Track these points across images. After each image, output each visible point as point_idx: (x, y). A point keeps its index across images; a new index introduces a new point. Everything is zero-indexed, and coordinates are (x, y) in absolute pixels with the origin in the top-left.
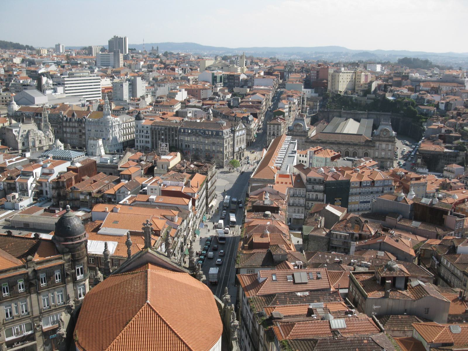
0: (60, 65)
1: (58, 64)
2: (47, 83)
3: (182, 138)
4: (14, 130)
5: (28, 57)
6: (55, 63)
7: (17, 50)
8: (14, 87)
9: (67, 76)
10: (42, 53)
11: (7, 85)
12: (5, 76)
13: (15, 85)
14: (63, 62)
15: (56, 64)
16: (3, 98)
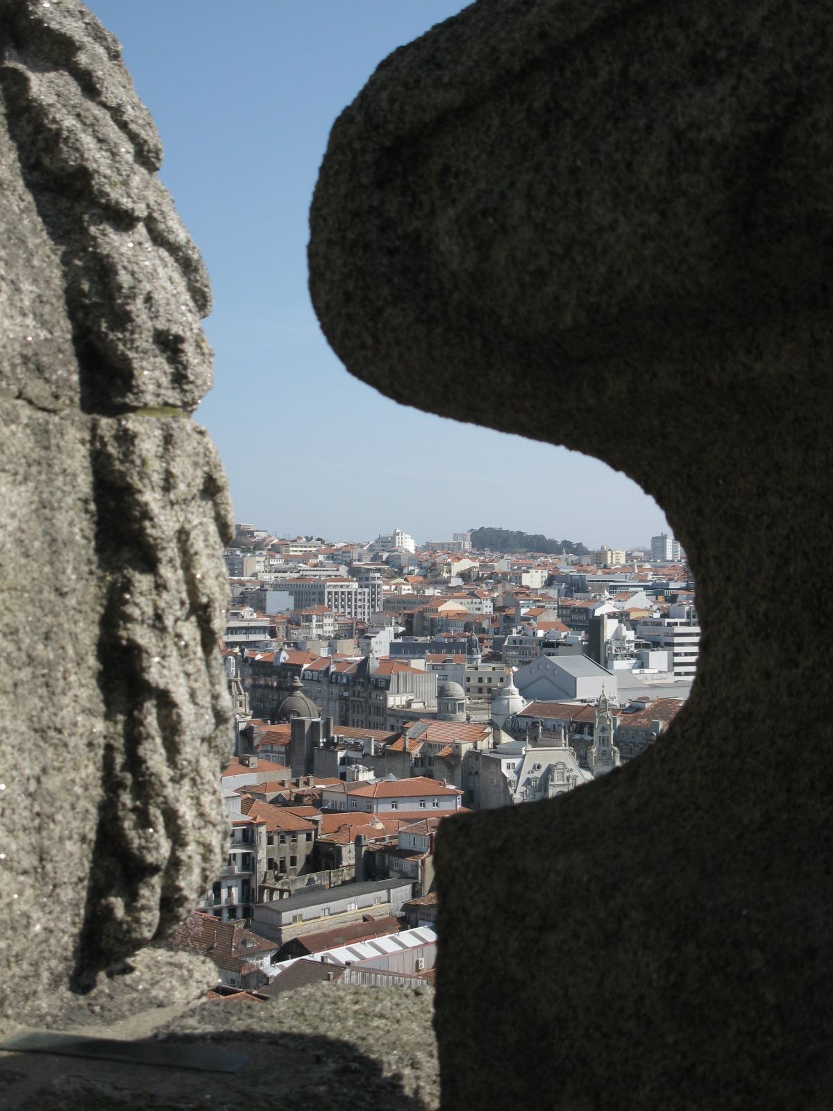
0: (661, 593)
1: (655, 590)
2: (618, 637)
4: (504, 762)
5: (566, 570)
6: (646, 588)
7: (535, 554)
8: (516, 648)
9: (684, 620)
10: (609, 561)
11: (497, 644)
12: (493, 620)
13: (521, 642)
14: (672, 585)
15: (650, 592)
16: (481, 680)
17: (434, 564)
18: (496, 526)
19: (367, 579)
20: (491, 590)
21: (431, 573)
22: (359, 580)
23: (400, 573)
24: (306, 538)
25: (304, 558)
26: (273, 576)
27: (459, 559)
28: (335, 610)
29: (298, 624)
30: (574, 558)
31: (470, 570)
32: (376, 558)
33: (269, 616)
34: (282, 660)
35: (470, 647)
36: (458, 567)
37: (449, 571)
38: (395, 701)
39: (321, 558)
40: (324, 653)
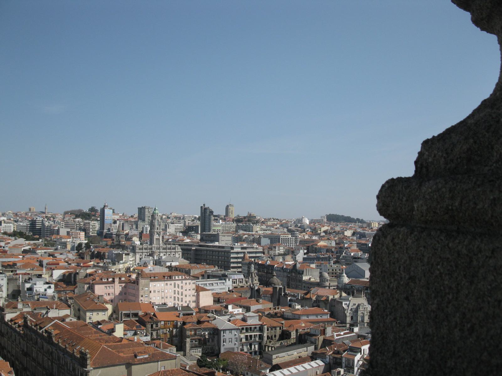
3: (216, 337)
4: (344, 303)
5: (359, 230)
7: (348, 223)
8: (344, 259)
10: (372, 226)
11: (338, 257)
12: (336, 248)
13: (346, 257)
16: (333, 270)
17: (315, 228)
18: (335, 213)
19: (294, 234)
20: (334, 237)
21: (314, 231)
22: (291, 234)
23: (304, 231)
24: (273, 219)
25: (272, 226)
26: (262, 232)
27: (324, 226)
28: (283, 244)
29: (272, 249)
30: (360, 224)
31: (327, 230)
32: (296, 226)
33: (262, 246)
34: (268, 264)
35: (329, 259)
36: (323, 229)
37: (320, 230)
38: (305, 278)
39: (278, 226)
40: (281, 260)
